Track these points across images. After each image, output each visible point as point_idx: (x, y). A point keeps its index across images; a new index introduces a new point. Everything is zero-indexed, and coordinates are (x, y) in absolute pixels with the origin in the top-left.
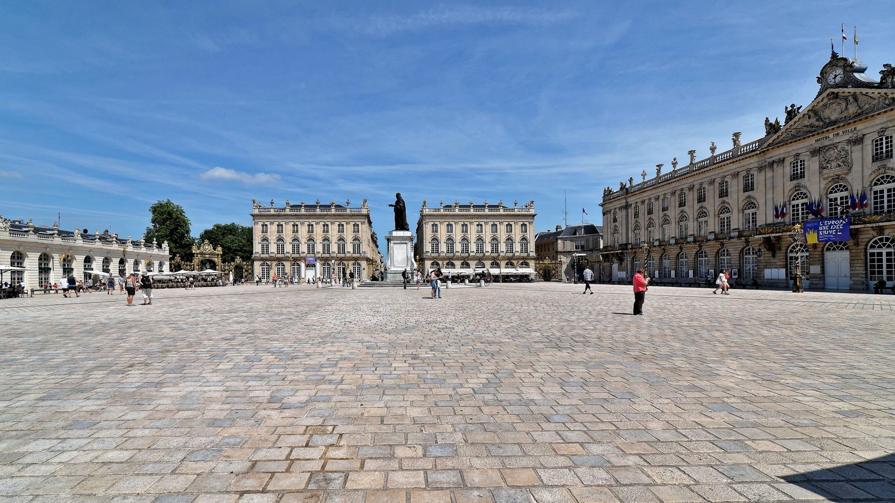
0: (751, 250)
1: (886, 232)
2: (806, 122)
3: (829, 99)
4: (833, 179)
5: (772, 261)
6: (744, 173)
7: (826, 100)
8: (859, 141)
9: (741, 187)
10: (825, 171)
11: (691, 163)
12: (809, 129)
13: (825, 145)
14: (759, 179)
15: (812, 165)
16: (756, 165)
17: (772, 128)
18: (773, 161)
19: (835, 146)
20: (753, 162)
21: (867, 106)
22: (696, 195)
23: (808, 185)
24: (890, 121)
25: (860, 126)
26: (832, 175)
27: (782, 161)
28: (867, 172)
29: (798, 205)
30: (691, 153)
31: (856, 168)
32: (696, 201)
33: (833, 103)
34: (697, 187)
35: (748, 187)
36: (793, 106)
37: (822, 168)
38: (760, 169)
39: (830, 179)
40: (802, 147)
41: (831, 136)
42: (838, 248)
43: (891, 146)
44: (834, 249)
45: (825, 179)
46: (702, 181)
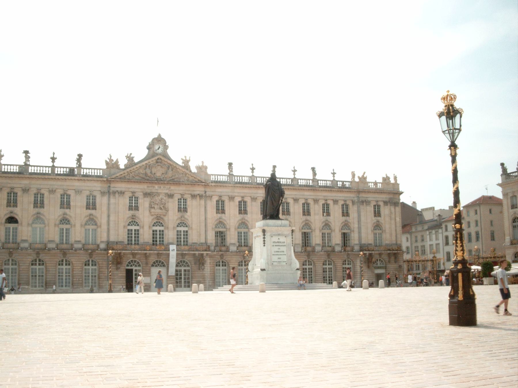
0: (64, 261)
1: (186, 257)
2: (141, 171)
3: (157, 162)
4: (157, 217)
5: (115, 272)
6: (88, 193)
7: (155, 161)
8: (171, 196)
9: (85, 204)
10: (153, 210)
11: (25, 163)
12: (144, 176)
13: (153, 191)
14: (102, 201)
15: (144, 203)
16: (99, 189)
17: (112, 165)
18: (117, 191)
19: (158, 194)
20: (97, 186)
21: (177, 176)
22: (32, 199)
23: (141, 217)
24: (187, 191)
25: (173, 188)
26: (157, 214)
27: (122, 193)
28: (176, 218)
29: (132, 230)
30: (26, 152)
31: (170, 213)
32: (32, 206)
33: (158, 165)
34: (33, 191)
35: (91, 205)
36: (131, 154)
37: (151, 207)
38: (103, 193)
39: (155, 216)
40: (139, 188)
41: (157, 187)
42: (158, 265)
43: (186, 205)
44: (156, 266)
45: (152, 215)
46: (42, 187)
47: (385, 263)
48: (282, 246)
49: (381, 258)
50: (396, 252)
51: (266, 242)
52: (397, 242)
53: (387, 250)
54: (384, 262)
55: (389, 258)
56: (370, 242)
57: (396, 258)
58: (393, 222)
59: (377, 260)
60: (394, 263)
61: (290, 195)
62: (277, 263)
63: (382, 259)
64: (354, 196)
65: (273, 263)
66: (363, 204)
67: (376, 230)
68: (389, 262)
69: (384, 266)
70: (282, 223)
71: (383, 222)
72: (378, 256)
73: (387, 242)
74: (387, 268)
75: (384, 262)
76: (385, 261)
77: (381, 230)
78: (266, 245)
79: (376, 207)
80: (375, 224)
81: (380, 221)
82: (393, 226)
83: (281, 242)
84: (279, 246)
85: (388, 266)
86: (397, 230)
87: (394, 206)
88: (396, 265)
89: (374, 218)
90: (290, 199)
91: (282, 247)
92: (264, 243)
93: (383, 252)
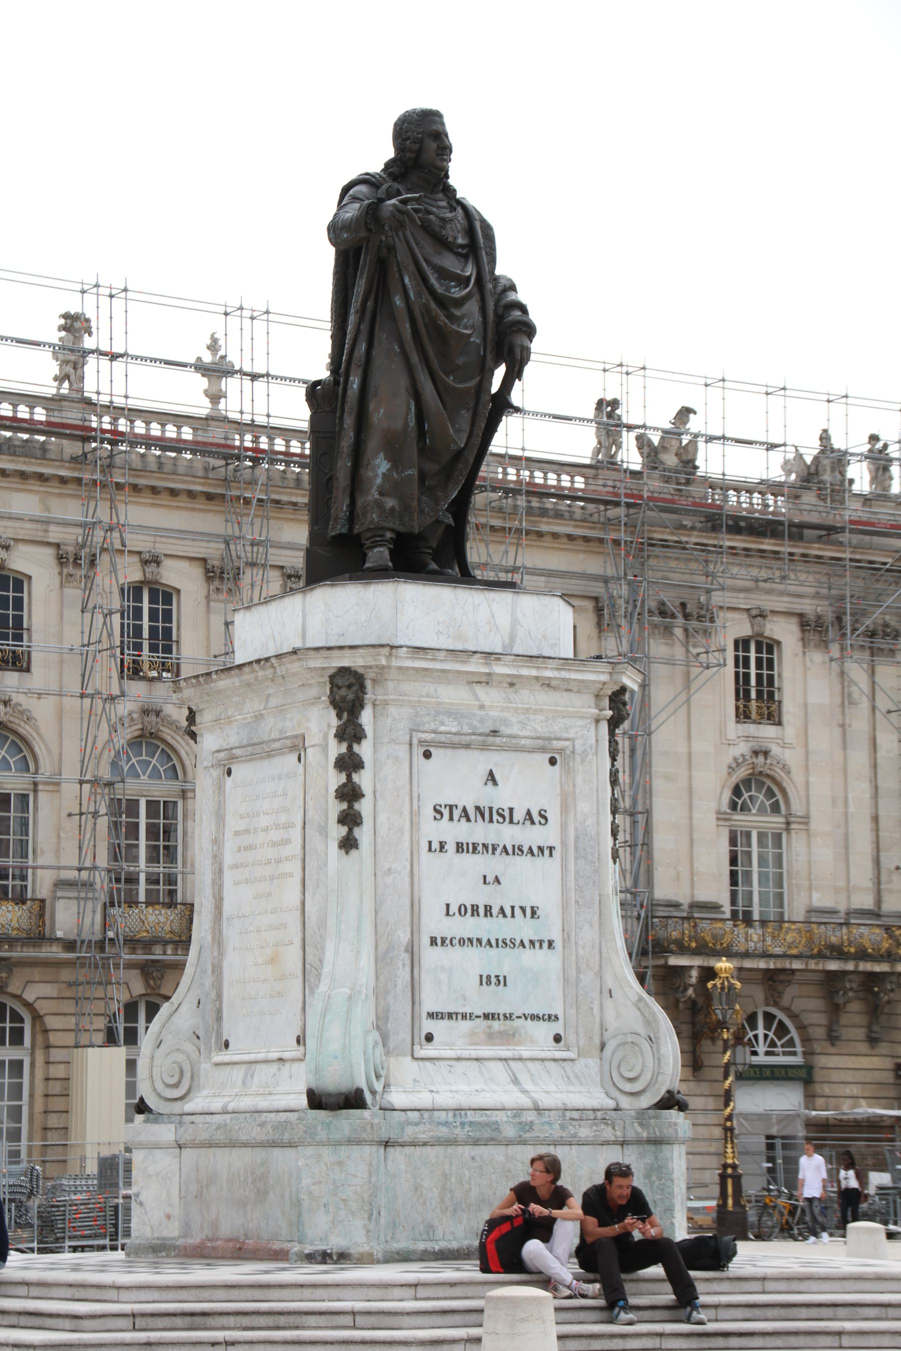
47: (806, 1040)
48: (518, 850)
49: (776, 1004)
50: (879, 968)
51: (364, 807)
52: (879, 902)
53: (820, 956)
54: (794, 1033)
55: (835, 1010)
56: (704, 895)
57: (875, 1011)
58: (859, 758)
59: (752, 1019)
60: (863, 1047)
61: (182, 534)
62: (466, 1025)
63: (781, 1015)
64: (610, 572)
65: (429, 1026)
66: (668, 630)
67: (745, 808)
68: (832, 1038)
69: (798, 1060)
70: (515, 623)
71: (791, 757)
72: (759, 993)
73: (821, 899)
74: (818, 1075)
75: (794, 1033)
76: (801, 1028)
77: (776, 808)
78: (363, 834)
79: (753, 655)
80: (742, 773)
81: (775, 750)
82: (861, 790)
83: (507, 815)
84: (490, 849)
85: (822, 1061)
86: (883, 822)
87: (866, 655)
88: (877, 1062)
89: (734, 730)
90: (184, 565)
91: (524, 861)
92: (350, 819)
93: (797, 965)
